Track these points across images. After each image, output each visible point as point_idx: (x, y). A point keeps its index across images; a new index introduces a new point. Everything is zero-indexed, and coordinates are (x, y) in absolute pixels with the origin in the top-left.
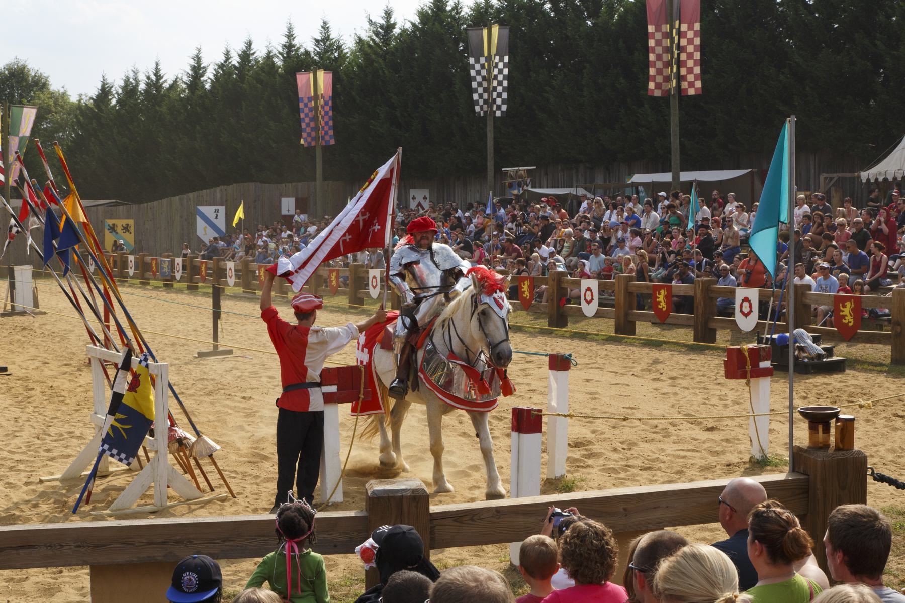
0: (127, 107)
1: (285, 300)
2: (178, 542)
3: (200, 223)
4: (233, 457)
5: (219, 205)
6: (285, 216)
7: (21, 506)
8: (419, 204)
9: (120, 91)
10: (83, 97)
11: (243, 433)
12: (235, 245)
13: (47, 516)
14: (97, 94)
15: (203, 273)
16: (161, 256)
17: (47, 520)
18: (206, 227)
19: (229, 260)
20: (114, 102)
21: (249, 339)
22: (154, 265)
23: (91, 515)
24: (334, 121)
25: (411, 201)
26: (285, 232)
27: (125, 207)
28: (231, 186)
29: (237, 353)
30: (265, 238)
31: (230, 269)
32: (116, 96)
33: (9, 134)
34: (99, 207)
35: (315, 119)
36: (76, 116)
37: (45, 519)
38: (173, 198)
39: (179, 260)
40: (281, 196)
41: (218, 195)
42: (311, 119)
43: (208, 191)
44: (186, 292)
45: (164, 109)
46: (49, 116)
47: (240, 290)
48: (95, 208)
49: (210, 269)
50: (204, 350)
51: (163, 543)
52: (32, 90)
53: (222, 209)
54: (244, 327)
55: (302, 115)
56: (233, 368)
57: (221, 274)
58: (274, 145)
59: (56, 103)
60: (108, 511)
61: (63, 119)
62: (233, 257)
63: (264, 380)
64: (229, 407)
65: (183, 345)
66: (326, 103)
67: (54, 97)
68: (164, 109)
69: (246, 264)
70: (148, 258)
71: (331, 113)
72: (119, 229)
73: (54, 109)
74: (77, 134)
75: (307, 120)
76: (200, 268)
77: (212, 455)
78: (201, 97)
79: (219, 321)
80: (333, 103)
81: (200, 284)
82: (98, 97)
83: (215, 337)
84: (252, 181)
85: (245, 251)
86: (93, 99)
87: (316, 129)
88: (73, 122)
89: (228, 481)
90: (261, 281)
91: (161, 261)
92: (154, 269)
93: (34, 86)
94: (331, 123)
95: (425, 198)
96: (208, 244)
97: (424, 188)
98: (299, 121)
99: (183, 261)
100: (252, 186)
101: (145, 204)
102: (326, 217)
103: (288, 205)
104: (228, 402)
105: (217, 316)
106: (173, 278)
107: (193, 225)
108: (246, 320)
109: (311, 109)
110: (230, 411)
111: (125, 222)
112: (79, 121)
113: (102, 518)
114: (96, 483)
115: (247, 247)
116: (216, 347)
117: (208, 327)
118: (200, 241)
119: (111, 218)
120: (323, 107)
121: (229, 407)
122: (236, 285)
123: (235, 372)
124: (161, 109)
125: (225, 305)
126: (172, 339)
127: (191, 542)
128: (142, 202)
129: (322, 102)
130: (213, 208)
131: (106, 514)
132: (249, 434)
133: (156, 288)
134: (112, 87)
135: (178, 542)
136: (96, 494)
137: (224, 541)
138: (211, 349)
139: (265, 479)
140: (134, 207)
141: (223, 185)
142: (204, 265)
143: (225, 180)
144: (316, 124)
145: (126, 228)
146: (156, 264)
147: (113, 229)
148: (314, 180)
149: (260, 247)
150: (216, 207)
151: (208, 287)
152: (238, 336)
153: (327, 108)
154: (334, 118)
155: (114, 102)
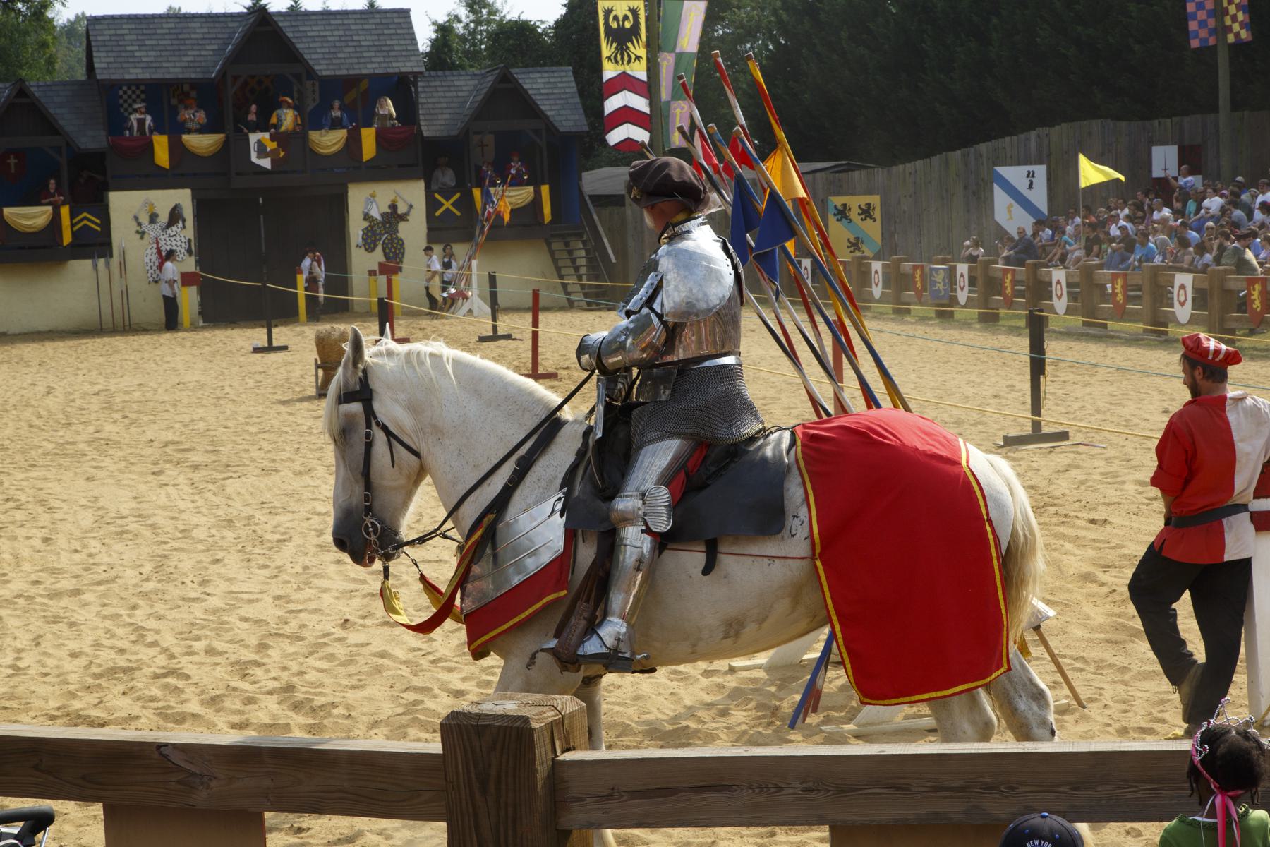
1: (1164, 338)
2: (990, 788)
4: (1078, 632)
5: (1036, 163)
6: (1159, 180)
7: (699, 714)
11: (1094, 588)
12: (1066, 237)
13: (745, 732)
15: (1009, 291)
16: (930, 261)
17: (745, 738)
18: (1011, 205)
19: (1056, 266)
21: (1098, 411)
22: (918, 276)
23: (822, 732)
26: (1160, 211)
27: (864, 172)
28: (1057, 127)
29: (1076, 437)
30: (1122, 223)
31: (1058, 282)
33: (660, 49)
34: (818, 175)
36: (775, 12)
37: (740, 738)
38: (951, 154)
39: (963, 268)
40: (1152, 142)
41: (1033, 144)
43: (1015, 138)
44: (978, 326)
46: (728, 14)
47: (1077, 321)
48: (811, 176)
49: (1020, 283)
50: (1014, 432)
51: (962, 789)
53: (1041, 171)
54: (1088, 390)
56: (1069, 465)
57: (1041, 290)
58: (1137, 47)
60: (851, 727)
61: (751, 19)
62: (1063, 260)
63: (1130, 488)
64: (1064, 537)
65: (976, 424)
69: (1088, 273)
70: (907, 266)
72: (854, 214)
74: (777, 44)
76: (1002, 282)
77: (1039, 627)
79: (1042, 379)
81: (1002, 311)
83: (1036, 408)
85: (1086, 248)
88: (770, 22)
89: (1070, 674)
90: (1115, 303)
91: (931, 269)
92: (919, 285)
96: (1017, 237)
99: (970, 269)
101: (901, 167)
103: (1164, 160)
104: (1062, 529)
105: (1038, 368)
106: (953, 301)
108: (1091, 376)
110: (1068, 546)
111: (863, 200)
112: (780, 21)
113: (840, 739)
114: (829, 674)
115: (1088, 239)
116: (1036, 426)
117: (1020, 390)
118: (1002, 233)
119: (839, 194)
121: (1064, 537)
122: (1069, 311)
123: (1074, 472)
125: (1053, 348)
126: (955, 412)
127: (1013, 788)
128: (894, 164)
131: (849, 732)
132: (1105, 590)
133: (923, 320)
135: (990, 788)
136: (829, 695)
137: (1075, 789)
138: (1028, 430)
139: (1139, 673)
140: (880, 174)
141: (1042, 127)
142: (1009, 276)
143: (1046, 118)
145: (866, 212)
146: (922, 276)
147: (842, 213)
149: (1113, 240)
150: (1030, 168)
151: (1018, 317)
152: (1077, 405)
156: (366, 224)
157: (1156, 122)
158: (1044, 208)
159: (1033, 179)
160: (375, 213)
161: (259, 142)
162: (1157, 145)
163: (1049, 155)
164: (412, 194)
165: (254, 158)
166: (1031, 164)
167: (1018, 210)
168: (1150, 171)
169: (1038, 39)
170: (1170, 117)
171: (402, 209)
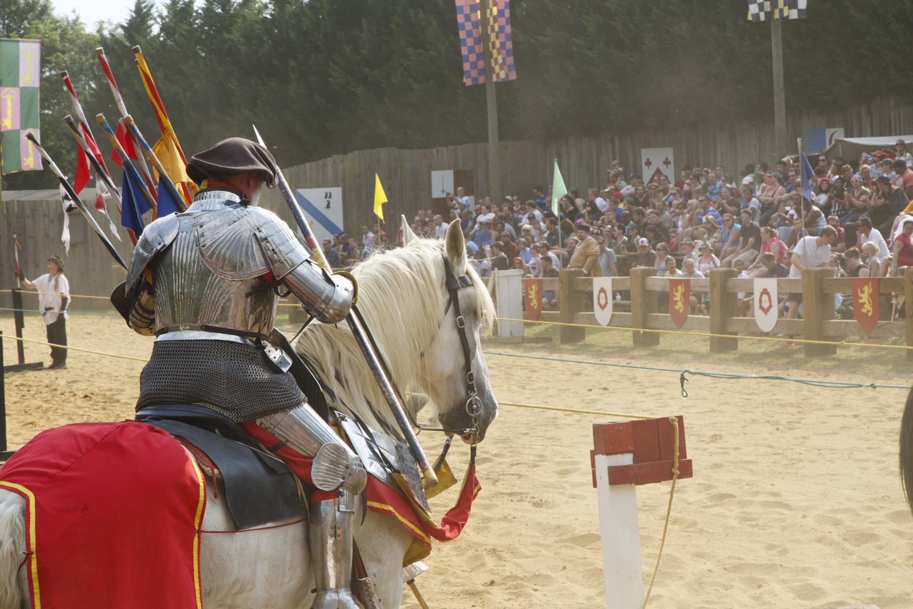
0: (176, 36)
5: (332, 186)
8: (658, 172)
9: (165, 13)
10: (105, 25)
14: (129, 18)
20: (156, 29)
24: (514, 43)
25: (645, 168)
28: (350, 155)
32: (159, 20)
35: (484, 39)
41: (330, 169)
42: (477, 41)
43: (314, 164)
45: (235, 36)
52: (26, 19)
53: (337, 192)
55: (462, 34)
58: (416, 86)
59: (63, 36)
61: (73, 61)
66: (501, 13)
67: (60, 27)
68: (235, 36)
71: (508, 29)
73: (58, 45)
75: (470, 42)
78: (295, 14)
80: (511, 13)
82: (131, 23)
84: (384, 146)
86: (122, 27)
87: (486, 55)
93: (29, 12)
94: (509, 45)
95: (667, 162)
97: (664, 145)
98: (456, 45)
100: (383, 152)
102: (508, 197)
109: (475, 25)
120: (495, 19)
124: (232, 37)
129: (495, 11)
130: (322, 191)
134: (152, 6)
144: (486, 48)
148: (485, 139)
150: (328, 190)
153: (503, 21)
154: (513, 37)
155: (156, 29)
157: (434, 150)
158: (341, 226)
159: (331, 200)
162: (435, 170)
163: (344, 179)
166: (328, 187)
168: (430, 193)
169: (330, 79)
170: (445, 145)
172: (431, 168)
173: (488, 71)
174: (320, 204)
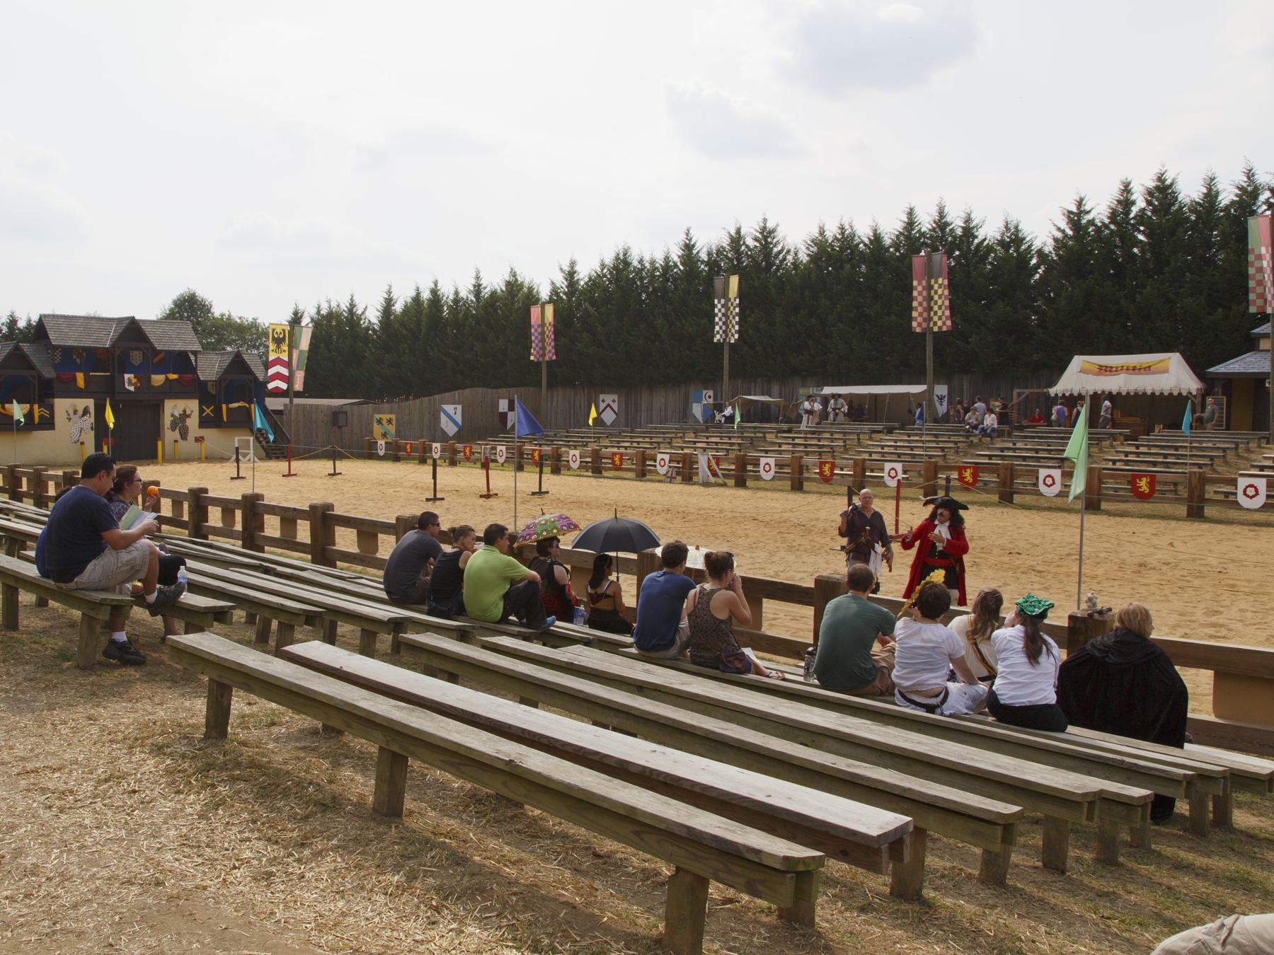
3: (443, 418)
41: (457, 396)
53: (459, 407)
72: (384, 422)
95: (614, 401)
107: (438, 420)
111: (389, 416)
118: (444, 433)
130: (454, 406)
145: (390, 421)
147: (380, 422)
156: (172, 419)
160: (177, 414)
161: (130, 380)
164: (193, 405)
165: (126, 386)
167: (450, 423)
171: (188, 413)
172: (499, 398)
173: (543, 355)
174: (451, 413)
